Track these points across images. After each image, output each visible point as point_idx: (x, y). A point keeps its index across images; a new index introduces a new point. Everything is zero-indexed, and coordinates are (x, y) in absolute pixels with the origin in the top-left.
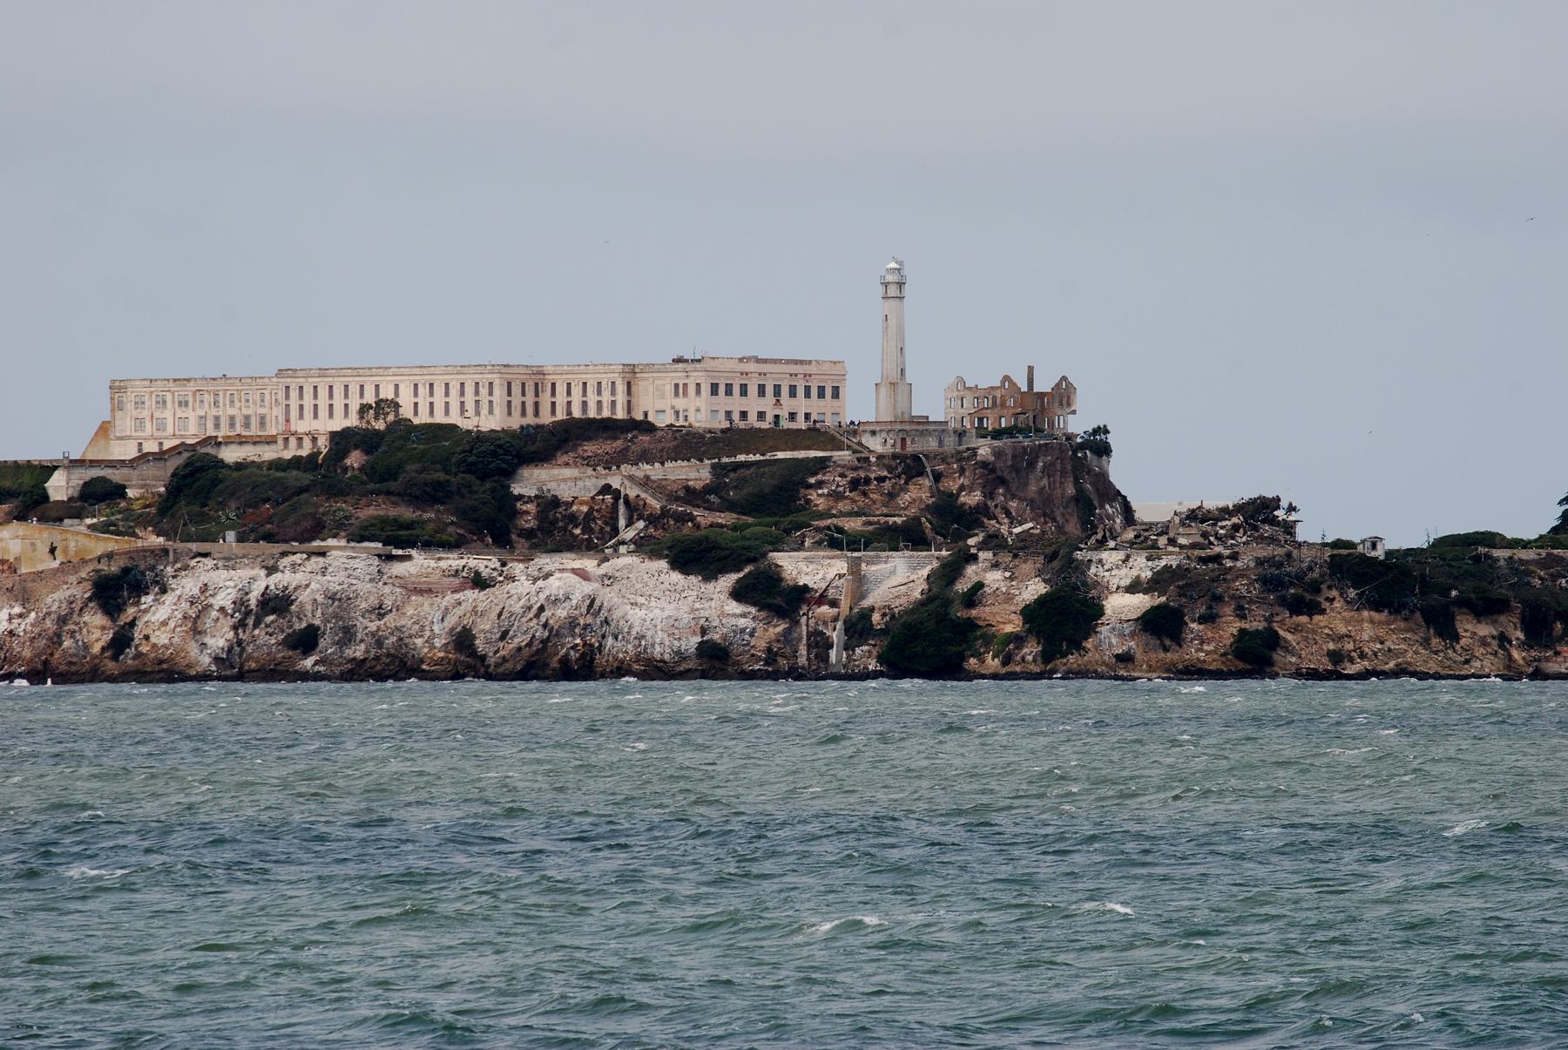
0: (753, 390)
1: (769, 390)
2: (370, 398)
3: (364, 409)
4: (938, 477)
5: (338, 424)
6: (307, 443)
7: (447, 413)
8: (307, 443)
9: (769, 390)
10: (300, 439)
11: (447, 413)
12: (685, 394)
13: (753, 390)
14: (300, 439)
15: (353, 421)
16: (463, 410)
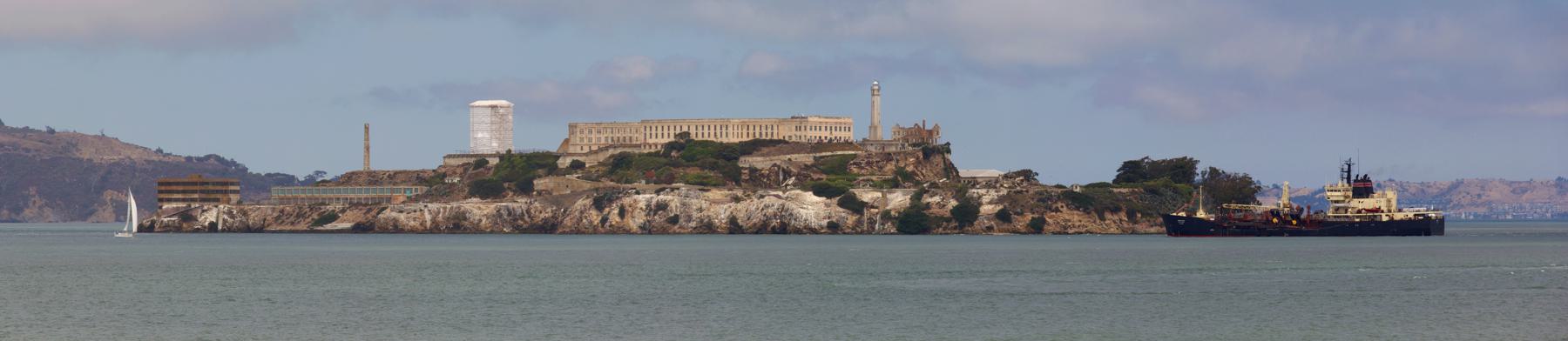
0: (823, 128)
1: (828, 128)
2: (678, 131)
3: (676, 136)
4: (898, 161)
5: (666, 140)
6: (653, 147)
7: (709, 136)
8: (653, 147)
9: (828, 128)
10: (650, 146)
11: (709, 136)
12: (800, 130)
13: (823, 128)
14: (650, 146)
15: (672, 139)
16: (715, 135)
